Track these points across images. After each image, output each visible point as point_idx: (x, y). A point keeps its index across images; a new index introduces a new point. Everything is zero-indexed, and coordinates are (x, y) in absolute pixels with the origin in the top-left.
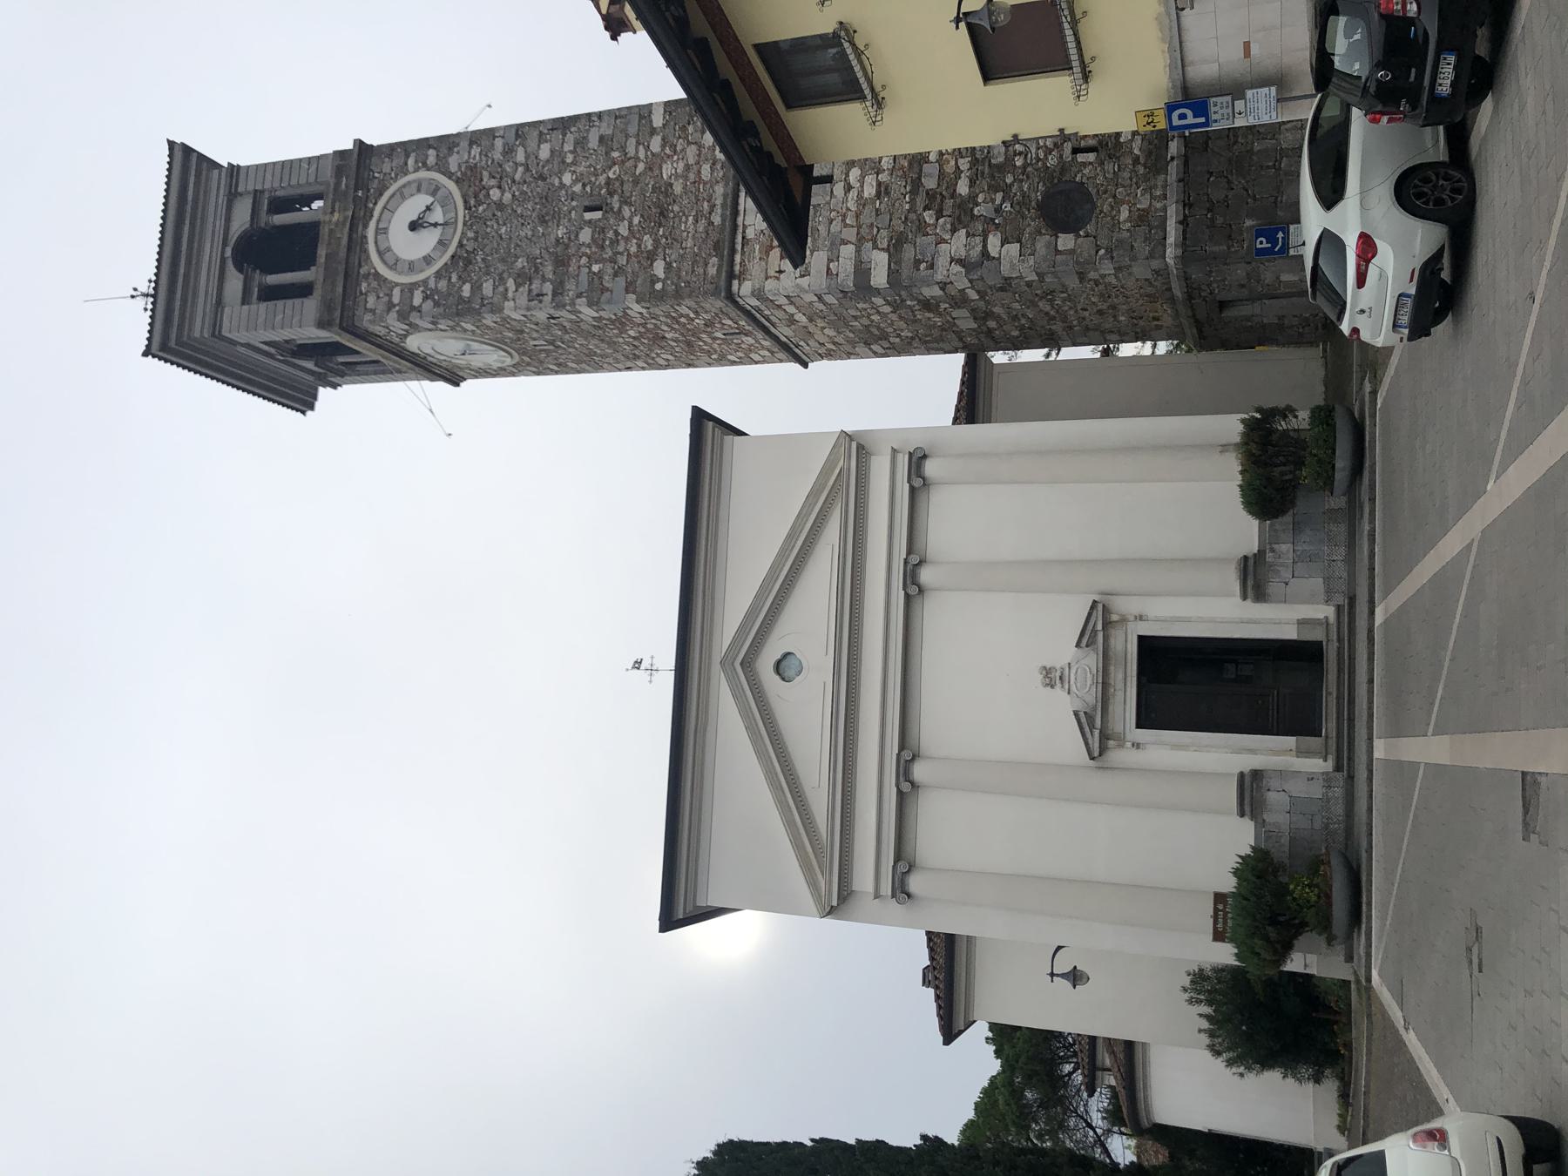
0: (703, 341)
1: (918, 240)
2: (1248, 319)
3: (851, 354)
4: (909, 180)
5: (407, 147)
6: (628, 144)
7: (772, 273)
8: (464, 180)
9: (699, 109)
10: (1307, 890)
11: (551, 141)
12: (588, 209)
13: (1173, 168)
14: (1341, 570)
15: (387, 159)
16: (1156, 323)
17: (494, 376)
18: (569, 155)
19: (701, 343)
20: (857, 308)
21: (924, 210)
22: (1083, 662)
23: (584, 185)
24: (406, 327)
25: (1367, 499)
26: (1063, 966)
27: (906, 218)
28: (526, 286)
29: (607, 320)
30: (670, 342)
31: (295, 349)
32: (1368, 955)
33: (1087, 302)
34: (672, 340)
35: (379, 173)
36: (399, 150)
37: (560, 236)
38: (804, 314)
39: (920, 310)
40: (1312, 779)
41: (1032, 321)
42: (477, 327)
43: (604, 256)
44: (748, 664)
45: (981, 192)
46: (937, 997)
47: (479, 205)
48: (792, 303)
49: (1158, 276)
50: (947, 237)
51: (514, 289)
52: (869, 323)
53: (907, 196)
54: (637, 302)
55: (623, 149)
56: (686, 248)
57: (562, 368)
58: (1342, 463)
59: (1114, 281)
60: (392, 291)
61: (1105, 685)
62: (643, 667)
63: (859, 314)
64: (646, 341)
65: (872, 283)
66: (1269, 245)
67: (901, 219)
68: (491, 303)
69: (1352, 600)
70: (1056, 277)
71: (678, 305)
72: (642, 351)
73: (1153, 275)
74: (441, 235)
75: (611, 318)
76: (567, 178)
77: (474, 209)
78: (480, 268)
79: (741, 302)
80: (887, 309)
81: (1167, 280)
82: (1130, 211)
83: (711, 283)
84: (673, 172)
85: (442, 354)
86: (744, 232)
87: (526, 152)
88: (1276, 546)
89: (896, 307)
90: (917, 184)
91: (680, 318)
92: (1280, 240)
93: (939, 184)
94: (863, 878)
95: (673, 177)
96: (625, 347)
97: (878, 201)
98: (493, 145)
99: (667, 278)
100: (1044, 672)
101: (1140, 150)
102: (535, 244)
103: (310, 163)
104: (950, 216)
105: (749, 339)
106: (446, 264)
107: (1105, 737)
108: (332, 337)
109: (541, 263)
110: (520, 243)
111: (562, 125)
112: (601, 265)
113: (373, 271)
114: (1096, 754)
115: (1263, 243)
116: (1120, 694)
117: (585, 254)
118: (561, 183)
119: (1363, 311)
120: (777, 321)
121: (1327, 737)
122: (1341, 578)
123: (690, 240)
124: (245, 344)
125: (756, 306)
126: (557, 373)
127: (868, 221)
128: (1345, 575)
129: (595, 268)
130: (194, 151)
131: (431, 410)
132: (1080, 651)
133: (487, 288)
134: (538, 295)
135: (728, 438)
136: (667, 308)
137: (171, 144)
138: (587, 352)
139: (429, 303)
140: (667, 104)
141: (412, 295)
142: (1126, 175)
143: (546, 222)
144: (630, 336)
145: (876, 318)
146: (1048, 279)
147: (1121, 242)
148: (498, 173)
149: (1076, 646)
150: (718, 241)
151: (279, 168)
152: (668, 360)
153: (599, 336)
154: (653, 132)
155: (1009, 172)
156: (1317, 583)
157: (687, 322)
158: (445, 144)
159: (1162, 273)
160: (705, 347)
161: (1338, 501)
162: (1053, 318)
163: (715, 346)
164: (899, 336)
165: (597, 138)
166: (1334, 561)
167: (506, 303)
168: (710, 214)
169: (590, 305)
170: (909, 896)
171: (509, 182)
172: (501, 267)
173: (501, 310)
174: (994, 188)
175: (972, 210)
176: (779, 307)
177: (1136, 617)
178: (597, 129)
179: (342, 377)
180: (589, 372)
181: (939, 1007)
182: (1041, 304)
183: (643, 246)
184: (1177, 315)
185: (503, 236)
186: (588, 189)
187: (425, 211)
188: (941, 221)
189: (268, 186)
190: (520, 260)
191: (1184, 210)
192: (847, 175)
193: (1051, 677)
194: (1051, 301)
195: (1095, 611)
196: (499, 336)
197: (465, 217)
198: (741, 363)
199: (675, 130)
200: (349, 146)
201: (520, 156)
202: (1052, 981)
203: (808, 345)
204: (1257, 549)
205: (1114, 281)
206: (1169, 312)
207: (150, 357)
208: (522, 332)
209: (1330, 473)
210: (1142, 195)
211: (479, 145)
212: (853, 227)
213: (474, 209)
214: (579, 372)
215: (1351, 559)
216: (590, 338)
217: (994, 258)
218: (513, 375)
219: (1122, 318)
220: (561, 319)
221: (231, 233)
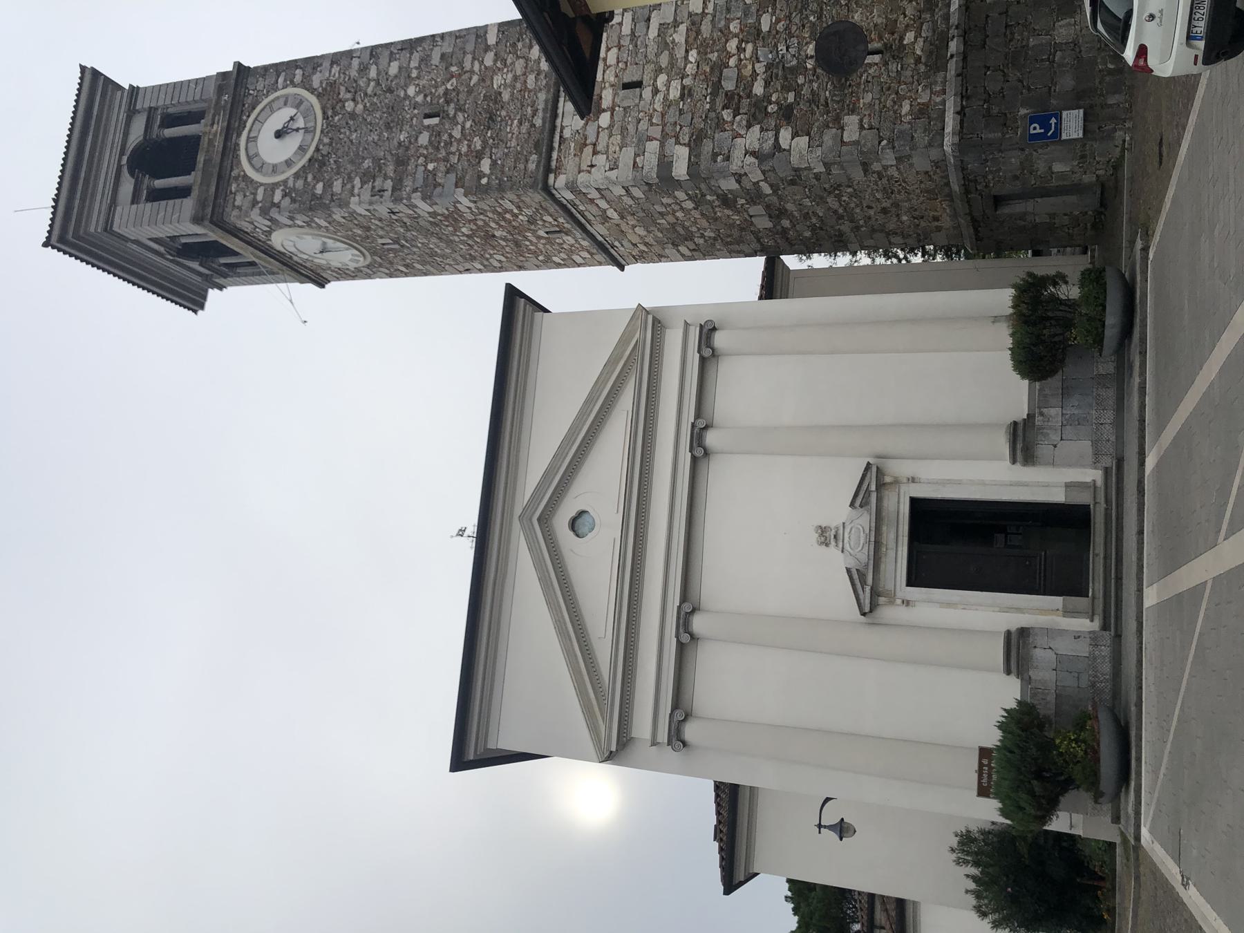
0: (529, 240)
1: (716, 135)
2: (1023, 216)
3: (662, 256)
4: (710, 84)
5: (278, 68)
6: (465, 60)
7: (584, 167)
8: (324, 95)
9: (531, 27)
10: (1073, 745)
11: (399, 59)
12: (428, 116)
13: (952, 66)
14: (1108, 432)
15: (261, 79)
16: (936, 223)
17: (354, 277)
18: (414, 71)
19: (528, 243)
20: (663, 204)
21: (723, 109)
22: (857, 521)
23: (426, 96)
24: (269, 223)
25: (1138, 351)
26: (830, 818)
27: (706, 117)
28: (371, 183)
29: (442, 215)
30: (500, 241)
31: (180, 247)
32: (1138, 813)
33: (871, 199)
34: (501, 239)
35: (254, 90)
36: (271, 70)
37: (402, 140)
38: (615, 210)
39: (719, 206)
40: (1079, 637)
41: (822, 221)
42: (330, 223)
43: (440, 156)
44: (545, 520)
45: (774, 92)
46: (721, 850)
47: (336, 116)
48: (603, 197)
49: (937, 168)
50: (742, 132)
51: (360, 186)
52: (675, 221)
53: (708, 97)
54: (466, 196)
55: (461, 64)
56: (510, 147)
57: (410, 271)
58: (1112, 320)
59: (896, 174)
60: (257, 190)
61: (878, 544)
62: (466, 534)
63: (664, 210)
64: (479, 240)
65: (673, 174)
66: (1042, 131)
67: (701, 117)
68: (339, 199)
69: (1120, 462)
70: (843, 168)
71: (501, 198)
72: (476, 251)
73: (932, 166)
74: (302, 141)
75: (444, 214)
76: (411, 91)
77: (330, 119)
78: (332, 168)
79: (558, 196)
80: (689, 205)
81: (946, 173)
82: (911, 105)
83: (531, 177)
84: (503, 82)
85: (304, 253)
86: (561, 132)
87: (378, 69)
88: (1045, 410)
89: (698, 201)
90: (717, 86)
91: (505, 214)
92: (1053, 125)
93: (736, 86)
94: (642, 726)
95: (502, 87)
96: (462, 246)
97: (681, 103)
98: (350, 64)
99: (492, 174)
100: (819, 531)
101: (922, 51)
102: (380, 146)
103: (197, 83)
104: (746, 114)
105: (569, 238)
106: (304, 166)
107: (875, 593)
108: (205, 235)
109: (384, 164)
110: (366, 146)
111: (410, 45)
112: (436, 164)
113: (242, 173)
114: (867, 609)
115: (1036, 129)
116: (891, 554)
117: (423, 155)
118: (406, 94)
119: (1152, 17)
120: (592, 218)
121: (1094, 598)
122: (1108, 440)
123: (514, 140)
124: (134, 240)
125: (571, 200)
126: (406, 275)
127: (672, 120)
128: (1113, 438)
129: (431, 167)
130: (103, 75)
131: (291, 301)
132: (854, 512)
133: (337, 186)
134: (379, 191)
135: (539, 315)
136: (491, 201)
137: (83, 69)
138: (427, 251)
139: (287, 199)
140: (501, 25)
141: (274, 193)
142: (909, 73)
143: (391, 128)
144: (464, 235)
145: (680, 214)
146: (835, 171)
147: (901, 132)
148: (353, 87)
149: (850, 506)
150: (538, 140)
151: (170, 90)
152: (500, 261)
153: (437, 234)
154: (487, 48)
155: (801, 74)
156: (1085, 446)
157: (512, 219)
158: (311, 64)
159: (939, 164)
160: (532, 247)
161: (1106, 366)
162: (841, 217)
163: (541, 246)
164: (702, 236)
165: (439, 56)
166: (1102, 424)
167: (352, 198)
168: (533, 117)
169: (424, 199)
170: (685, 744)
171: (362, 95)
172: (349, 166)
173: (347, 204)
174: (786, 88)
175: (766, 108)
176: (592, 201)
177: (909, 479)
178: (439, 47)
179: (225, 278)
180: (433, 274)
181: (722, 859)
182: (829, 200)
183: (473, 147)
184: (955, 215)
185: (354, 141)
186: (429, 99)
187: (289, 121)
188: (738, 118)
189: (161, 103)
190: (366, 162)
191: (962, 101)
192: (655, 81)
193: (826, 536)
194: (839, 197)
195: (869, 473)
196: (350, 233)
197: (322, 126)
198: (566, 266)
199: (506, 46)
200: (229, 68)
201: (373, 73)
202: (820, 833)
203: (622, 245)
204: (1026, 412)
205: (896, 174)
206: (948, 211)
207: (50, 247)
208: (368, 229)
209: (1100, 330)
210: (923, 90)
211: (338, 65)
212: (658, 125)
213: (330, 119)
214: (426, 274)
215: (1119, 424)
216: (429, 236)
217: (784, 150)
218: (369, 276)
219: (905, 218)
220: (400, 215)
221: (128, 146)
